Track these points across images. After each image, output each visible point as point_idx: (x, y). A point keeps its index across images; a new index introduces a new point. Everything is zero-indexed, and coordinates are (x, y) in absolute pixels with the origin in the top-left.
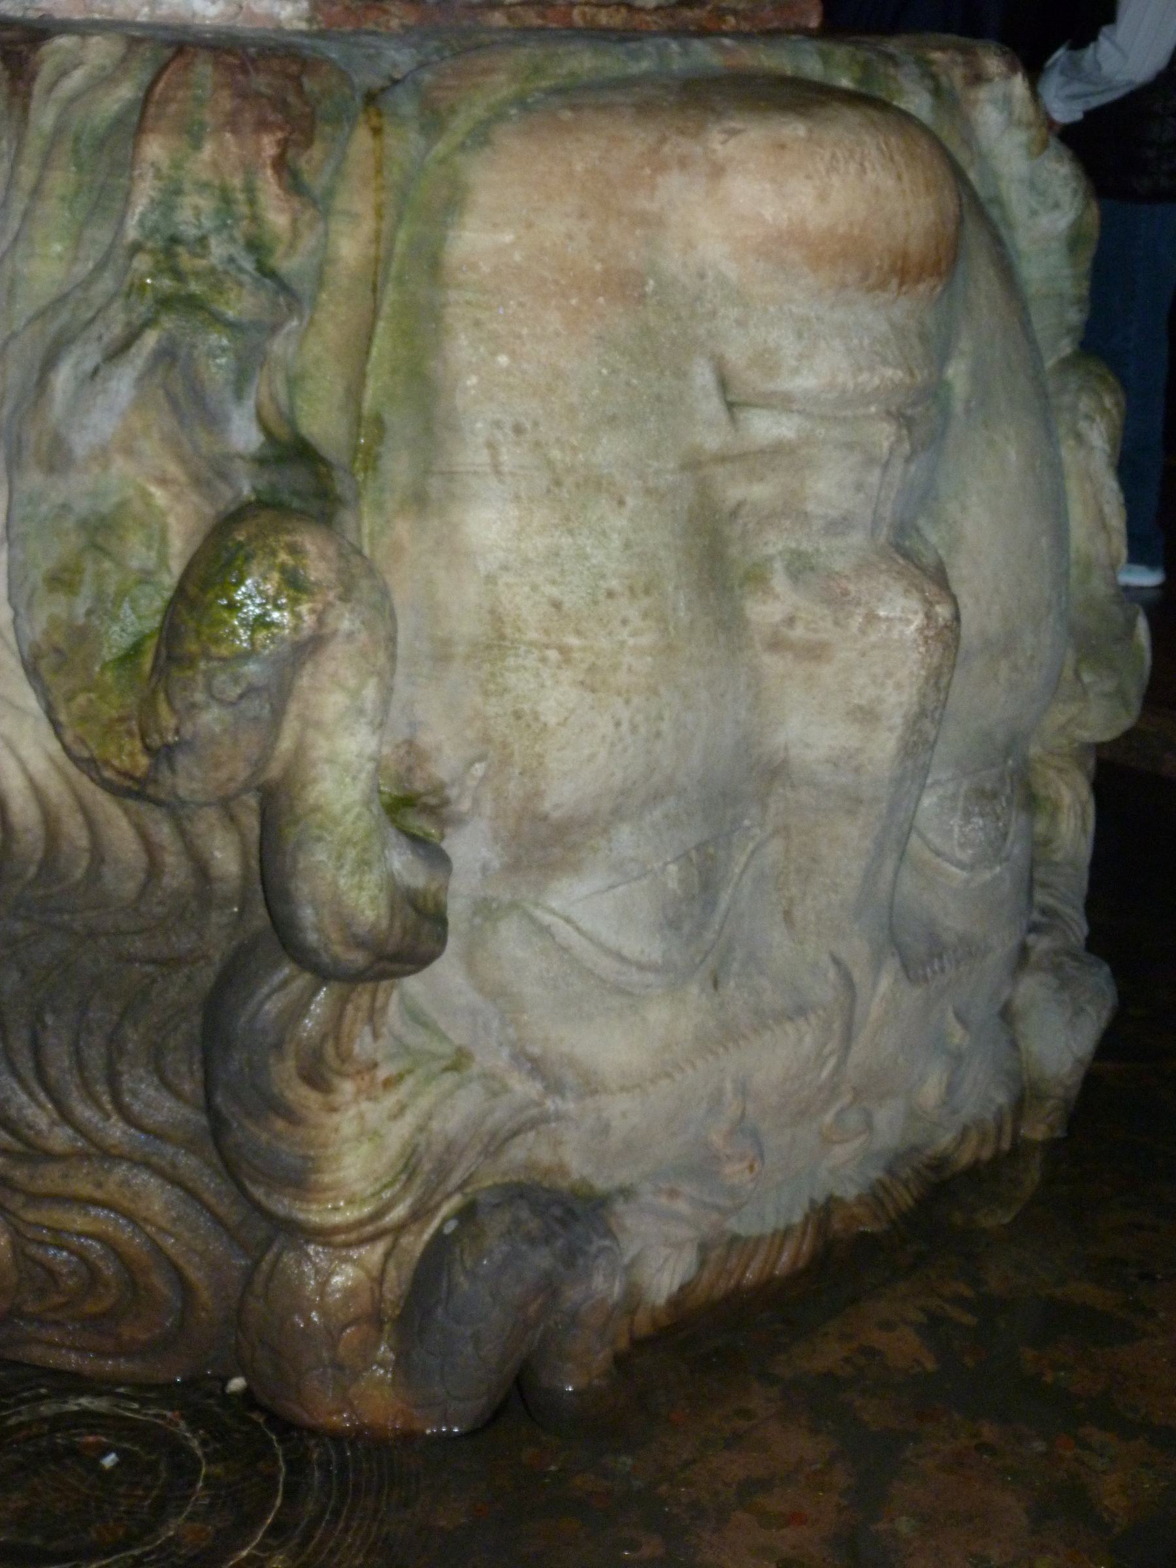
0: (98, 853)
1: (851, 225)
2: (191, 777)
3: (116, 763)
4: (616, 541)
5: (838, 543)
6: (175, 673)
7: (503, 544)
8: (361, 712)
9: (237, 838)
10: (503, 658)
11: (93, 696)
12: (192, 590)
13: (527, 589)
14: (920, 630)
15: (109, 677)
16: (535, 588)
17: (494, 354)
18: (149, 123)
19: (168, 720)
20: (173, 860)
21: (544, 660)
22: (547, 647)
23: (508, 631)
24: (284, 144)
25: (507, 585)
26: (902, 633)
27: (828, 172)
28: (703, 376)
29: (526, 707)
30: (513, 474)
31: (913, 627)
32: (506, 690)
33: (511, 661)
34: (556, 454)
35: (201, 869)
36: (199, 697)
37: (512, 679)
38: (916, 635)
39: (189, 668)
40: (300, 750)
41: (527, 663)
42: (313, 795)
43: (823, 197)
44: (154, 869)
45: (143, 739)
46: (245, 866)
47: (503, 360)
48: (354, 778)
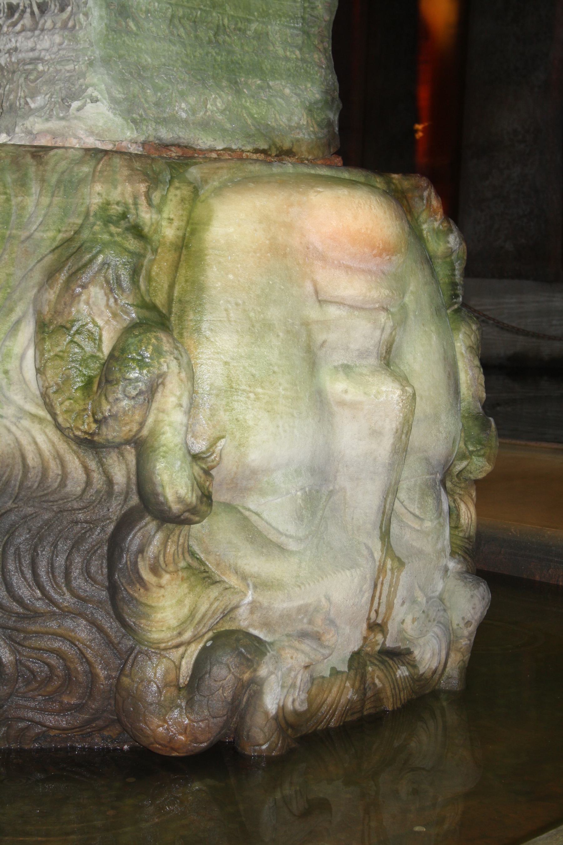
0: (65, 476)
1: (367, 229)
2: (114, 430)
3: (82, 428)
5: (364, 362)
6: (109, 388)
7: (232, 349)
8: (181, 405)
9: (124, 466)
11: (72, 401)
12: (117, 354)
13: (241, 368)
14: (400, 396)
15: (78, 394)
16: (244, 368)
17: (227, 274)
19: (106, 407)
20: (97, 476)
21: (248, 397)
22: (250, 392)
23: (234, 385)
24: (149, 188)
25: (234, 366)
26: (392, 398)
27: (357, 208)
28: (309, 288)
29: (241, 417)
30: (235, 322)
31: (396, 395)
32: (233, 409)
33: (235, 398)
34: (252, 314)
35: (110, 482)
36: (120, 396)
37: (236, 405)
38: (398, 398)
39: (116, 384)
40: (157, 422)
41: (242, 399)
42: (163, 439)
44: (88, 483)
45: (94, 417)
46: (129, 478)
48: (179, 433)
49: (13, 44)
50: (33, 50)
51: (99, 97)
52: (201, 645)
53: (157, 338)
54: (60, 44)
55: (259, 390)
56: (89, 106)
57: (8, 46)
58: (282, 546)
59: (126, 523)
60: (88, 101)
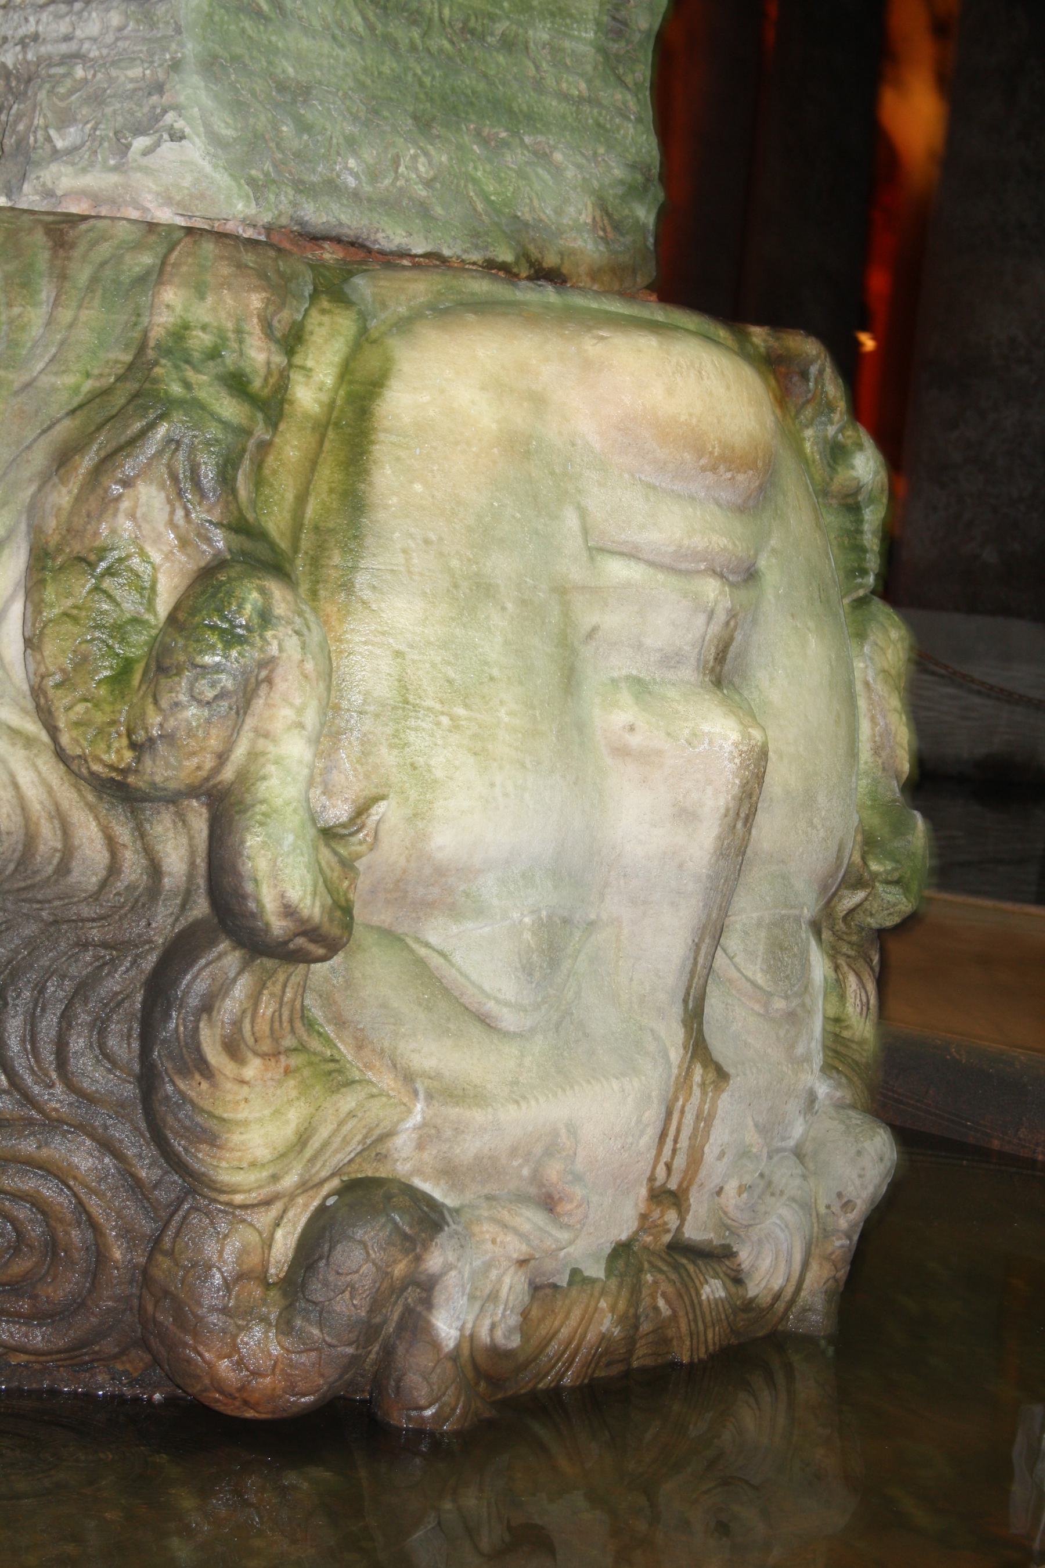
0: (68, 852)
1: (691, 415)
2: (168, 765)
3: (105, 757)
4: (499, 639)
5: (670, 675)
6: (163, 681)
7: (410, 628)
8: (301, 726)
9: (185, 841)
10: (406, 718)
11: (89, 705)
12: (181, 616)
13: (428, 665)
15: (103, 691)
16: (434, 665)
17: (411, 482)
18: (165, 278)
19: (154, 719)
21: (438, 724)
22: (443, 713)
23: (411, 698)
25: (413, 661)
26: (721, 747)
27: (674, 373)
29: (421, 761)
30: (421, 574)
31: (730, 742)
32: (406, 745)
33: (412, 723)
34: (455, 563)
35: (155, 870)
36: (183, 698)
37: (412, 736)
38: (732, 748)
39: (176, 675)
40: (254, 755)
41: (424, 725)
42: (262, 789)
43: (670, 392)
44: (114, 869)
45: (129, 736)
46: (192, 865)
47: (418, 487)
48: (294, 779)
49: (31, 28)
50: (67, 38)
51: (187, 130)
52: (316, 1203)
53: (262, 591)
54: (120, 29)
55: (461, 711)
56: (168, 147)
57: (22, 32)
58: (487, 1021)
59: (183, 949)
60: (166, 136)
